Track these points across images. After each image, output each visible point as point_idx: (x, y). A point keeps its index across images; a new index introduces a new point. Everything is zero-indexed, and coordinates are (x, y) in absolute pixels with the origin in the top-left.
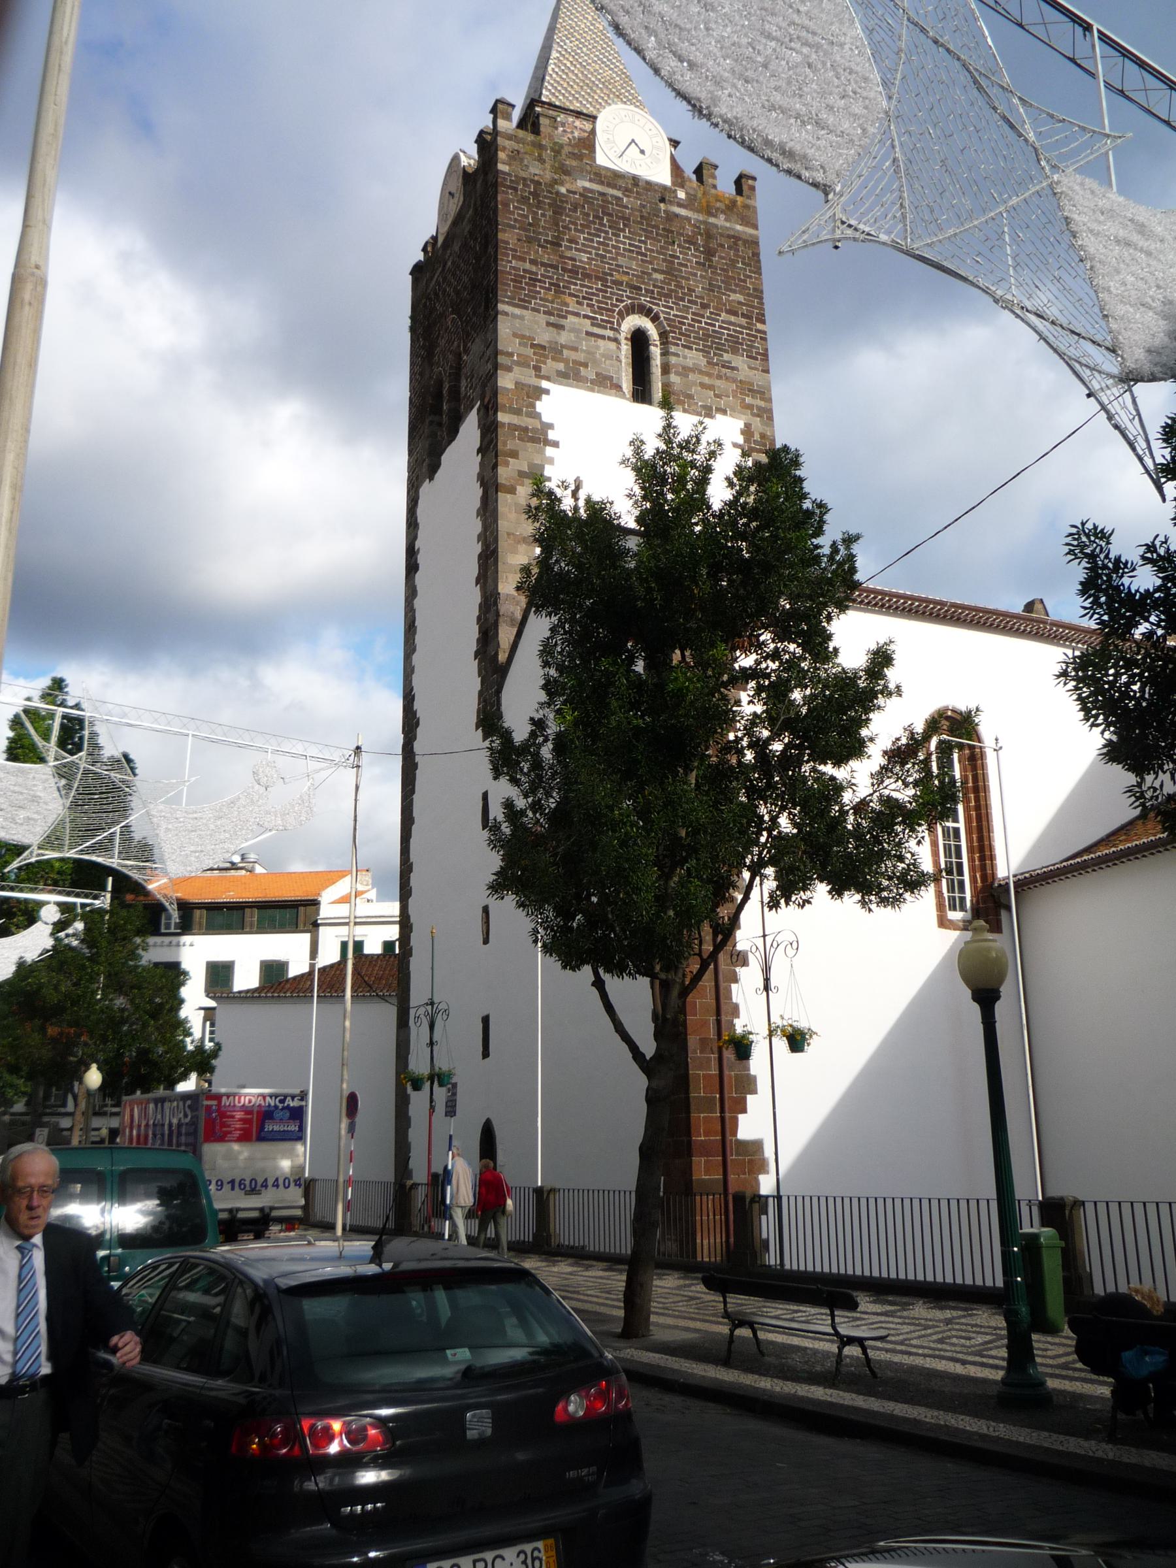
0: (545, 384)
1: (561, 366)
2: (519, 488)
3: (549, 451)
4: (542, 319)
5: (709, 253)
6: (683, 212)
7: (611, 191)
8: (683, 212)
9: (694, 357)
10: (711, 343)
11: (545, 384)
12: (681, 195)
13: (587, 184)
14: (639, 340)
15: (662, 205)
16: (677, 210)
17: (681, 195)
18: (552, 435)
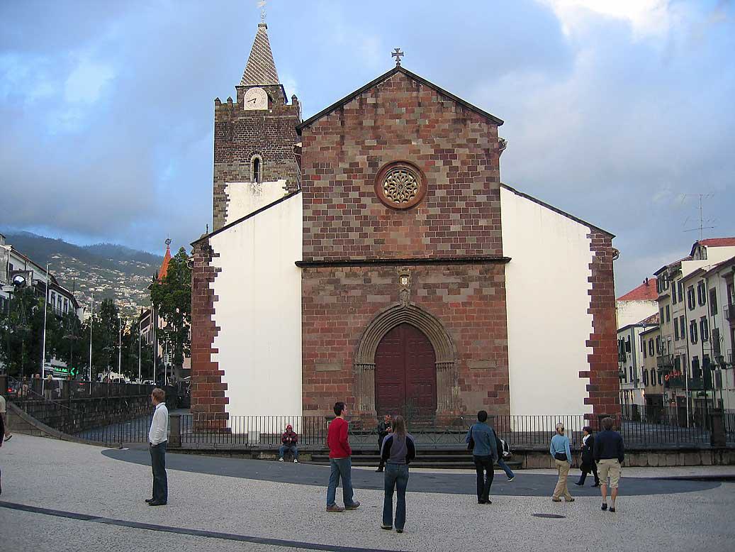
0: (226, 183)
1: (231, 177)
2: (219, 215)
3: (227, 203)
4: (226, 164)
5: (279, 128)
6: (271, 117)
7: (249, 118)
8: (271, 117)
9: (272, 163)
10: (277, 157)
11: (226, 183)
12: (271, 111)
13: (241, 118)
14: (257, 161)
15: (265, 117)
16: (269, 117)
17: (271, 111)
18: (228, 198)
